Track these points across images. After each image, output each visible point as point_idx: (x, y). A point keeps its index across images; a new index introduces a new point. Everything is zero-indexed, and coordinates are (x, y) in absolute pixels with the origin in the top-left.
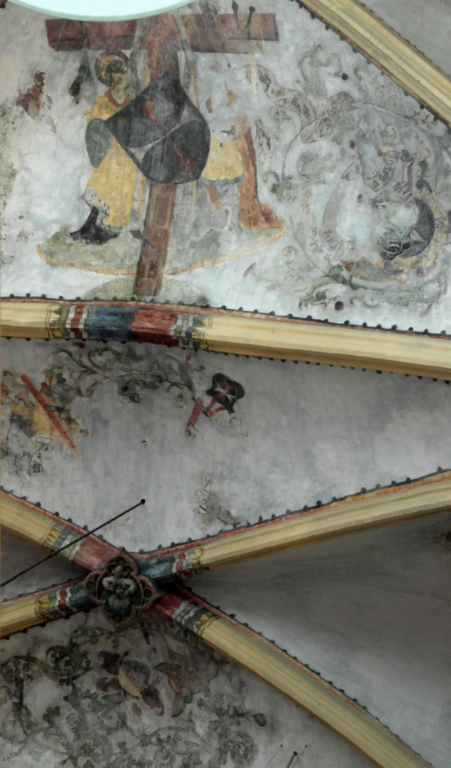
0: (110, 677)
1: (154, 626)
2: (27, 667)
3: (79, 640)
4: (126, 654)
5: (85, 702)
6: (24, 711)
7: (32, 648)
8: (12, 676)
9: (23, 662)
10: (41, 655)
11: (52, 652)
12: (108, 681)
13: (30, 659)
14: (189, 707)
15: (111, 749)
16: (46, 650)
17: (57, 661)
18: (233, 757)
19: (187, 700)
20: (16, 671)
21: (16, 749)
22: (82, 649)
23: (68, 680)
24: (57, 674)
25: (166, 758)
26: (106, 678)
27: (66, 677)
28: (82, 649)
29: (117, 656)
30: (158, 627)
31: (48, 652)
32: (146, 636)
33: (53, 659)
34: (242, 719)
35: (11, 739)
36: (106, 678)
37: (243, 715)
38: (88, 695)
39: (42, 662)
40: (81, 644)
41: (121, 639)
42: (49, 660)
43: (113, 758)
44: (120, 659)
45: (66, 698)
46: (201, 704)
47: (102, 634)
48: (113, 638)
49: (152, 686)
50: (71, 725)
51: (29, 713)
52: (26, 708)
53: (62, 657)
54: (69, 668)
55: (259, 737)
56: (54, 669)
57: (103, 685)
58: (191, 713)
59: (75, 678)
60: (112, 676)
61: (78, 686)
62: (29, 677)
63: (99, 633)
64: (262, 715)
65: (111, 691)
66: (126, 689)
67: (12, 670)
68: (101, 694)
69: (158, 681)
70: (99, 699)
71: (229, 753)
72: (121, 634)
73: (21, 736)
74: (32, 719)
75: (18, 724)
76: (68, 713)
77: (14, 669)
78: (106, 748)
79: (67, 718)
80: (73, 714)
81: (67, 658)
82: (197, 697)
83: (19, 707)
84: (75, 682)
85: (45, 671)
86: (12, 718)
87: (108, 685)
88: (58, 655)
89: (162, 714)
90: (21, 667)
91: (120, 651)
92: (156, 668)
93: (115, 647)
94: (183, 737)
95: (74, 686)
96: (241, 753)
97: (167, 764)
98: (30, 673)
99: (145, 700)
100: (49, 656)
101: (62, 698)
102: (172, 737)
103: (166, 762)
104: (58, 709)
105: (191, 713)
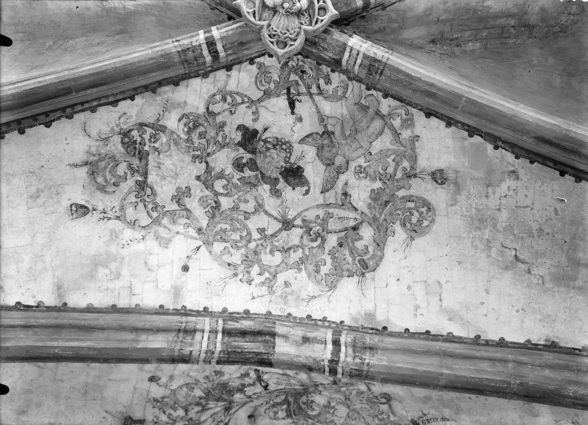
0: (247, 156)
1: (303, 89)
2: (154, 138)
3: (216, 108)
4: (265, 129)
5: (219, 185)
6: (149, 191)
7: (162, 113)
8: (135, 148)
9: (149, 131)
10: (172, 122)
11: (185, 120)
12: (244, 161)
13: (159, 128)
14: (343, 178)
15: (249, 233)
16: (178, 117)
17: (190, 131)
18: (404, 225)
19: (339, 171)
20: (140, 143)
21: (138, 235)
22: (219, 119)
23: (201, 157)
24: (189, 147)
25: (316, 240)
26: (243, 157)
27: (199, 153)
28: (219, 119)
29: (256, 132)
30: (309, 87)
31: (180, 120)
32: (292, 105)
33: (186, 130)
34: (413, 181)
35: (133, 224)
36: (243, 157)
37: (415, 176)
38: (221, 176)
39: (172, 132)
40: (219, 114)
41: (262, 111)
42: (181, 130)
43: (252, 245)
44: (258, 135)
45: (198, 178)
46: (360, 171)
47: (243, 103)
48: (254, 109)
49: (295, 164)
50: (204, 208)
51: (154, 193)
52: (152, 189)
53: (195, 127)
54: (203, 141)
55: (438, 196)
56: (187, 141)
57: (239, 166)
58: (346, 184)
59: (209, 155)
60: (249, 156)
61: (212, 164)
62: (156, 149)
63: (239, 100)
64: (441, 171)
65: (248, 173)
66: (263, 170)
67: (135, 142)
68: (237, 175)
69: (302, 157)
70: (235, 180)
71: (398, 223)
72: (262, 104)
73: (145, 221)
74: (158, 200)
75: (141, 205)
76: (201, 195)
77: (139, 139)
78: (244, 234)
79: (200, 199)
80: (207, 196)
81: (201, 129)
82: (353, 165)
83: (142, 185)
84: (209, 159)
85: (176, 144)
86: (134, 199)
87: (245, 165)
88: (191, 125)
89: (307, 192)
90: (147, 137)
91: (259, 126)
92: (302, 141)
93: (255, 120)
94: (335, 213)
95: (207, 163)
96: (414, 220)
97: (319, 246)
98: (157, 145)
99: (287, 181)
100: (181, 126)
101: (193, 177)
102: (321, 217)
103: (315, 244)
104: (188, 189)
105: (346, 184)
